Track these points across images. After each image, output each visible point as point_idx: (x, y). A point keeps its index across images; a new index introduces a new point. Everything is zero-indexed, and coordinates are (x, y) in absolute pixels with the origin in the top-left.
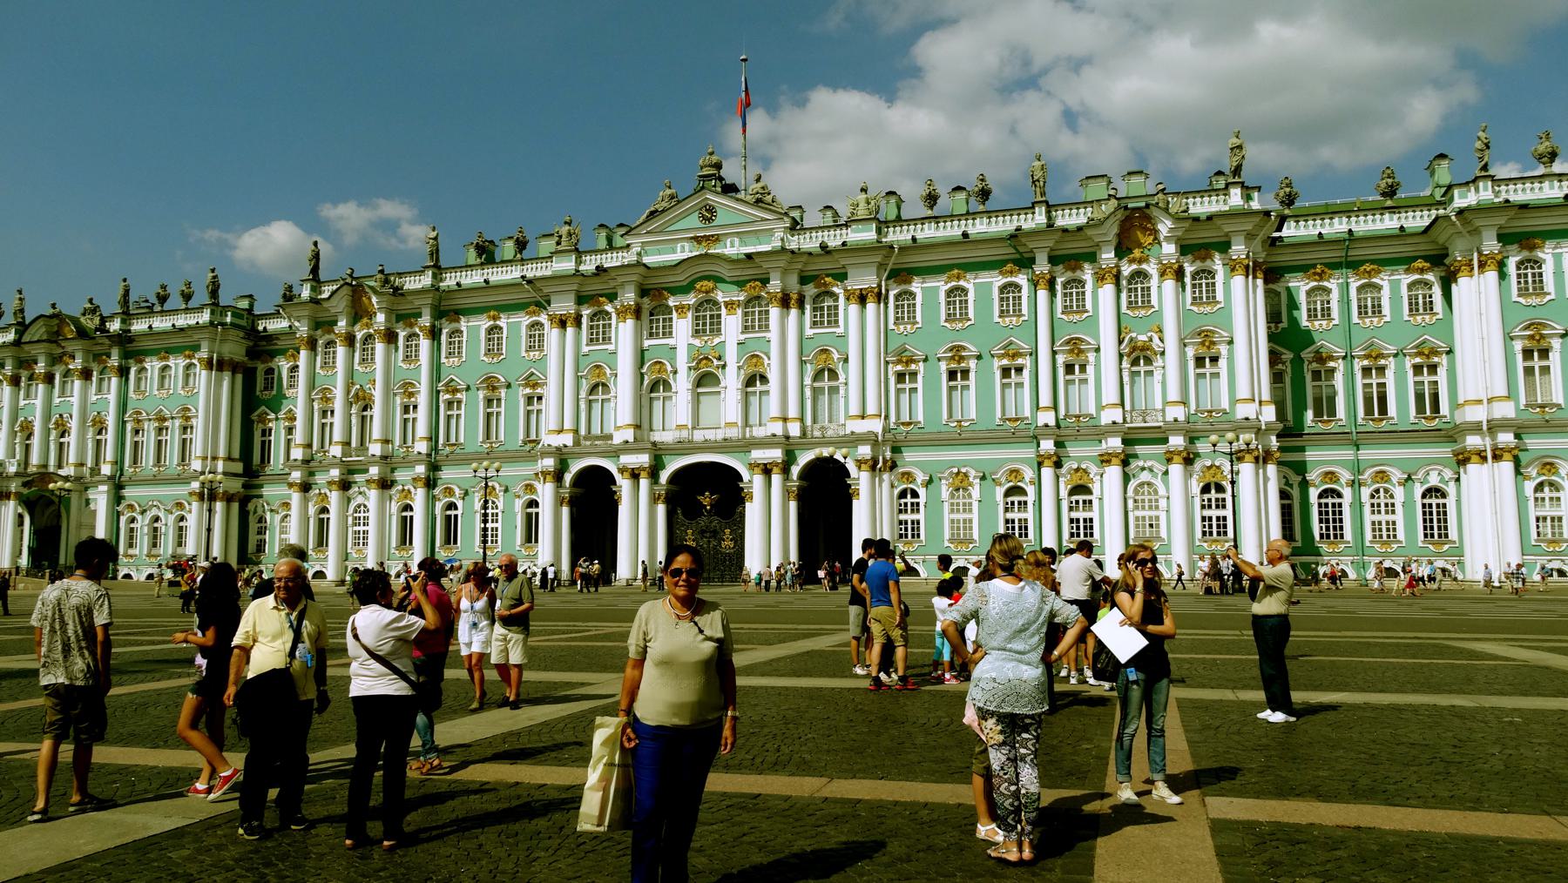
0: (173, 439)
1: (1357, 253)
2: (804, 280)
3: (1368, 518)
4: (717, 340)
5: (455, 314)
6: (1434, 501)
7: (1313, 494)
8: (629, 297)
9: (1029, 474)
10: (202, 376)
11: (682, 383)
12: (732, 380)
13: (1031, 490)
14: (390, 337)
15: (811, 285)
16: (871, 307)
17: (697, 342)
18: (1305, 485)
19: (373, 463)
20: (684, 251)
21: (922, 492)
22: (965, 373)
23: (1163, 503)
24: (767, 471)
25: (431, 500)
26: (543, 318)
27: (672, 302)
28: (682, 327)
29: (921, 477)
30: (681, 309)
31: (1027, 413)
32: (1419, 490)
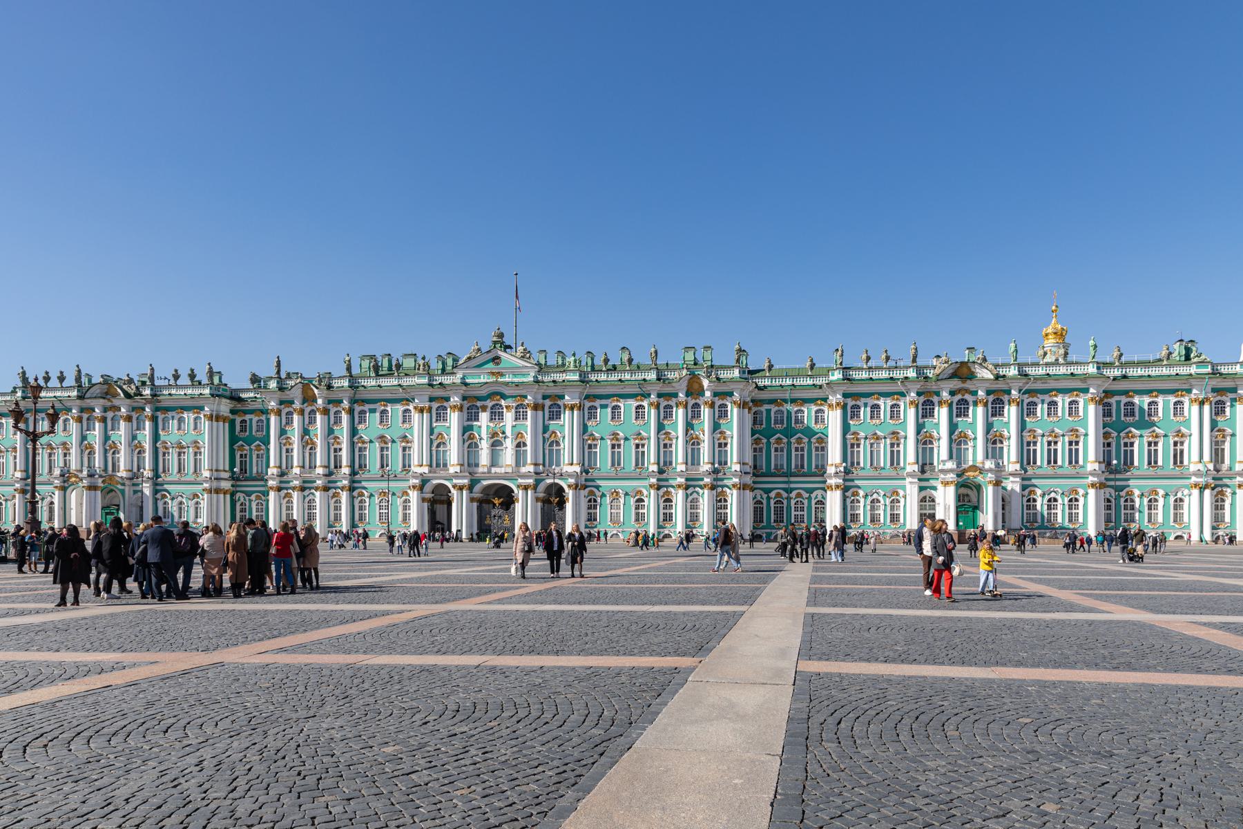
0: (189, 458)
2: (544, 397)
3: (793, 513)
7: (772, 502)
8: (455, 400)
9: (645, 492)
10: (205, 425)
14: (326, 412)
18: (769, 498)
19: (319, 478)
20: (483, 379)
22: (619, 446)
26: (411, 407)
27: (479, 404)
28: (484, 416)
30: (484, 409)
32: (813, 502)
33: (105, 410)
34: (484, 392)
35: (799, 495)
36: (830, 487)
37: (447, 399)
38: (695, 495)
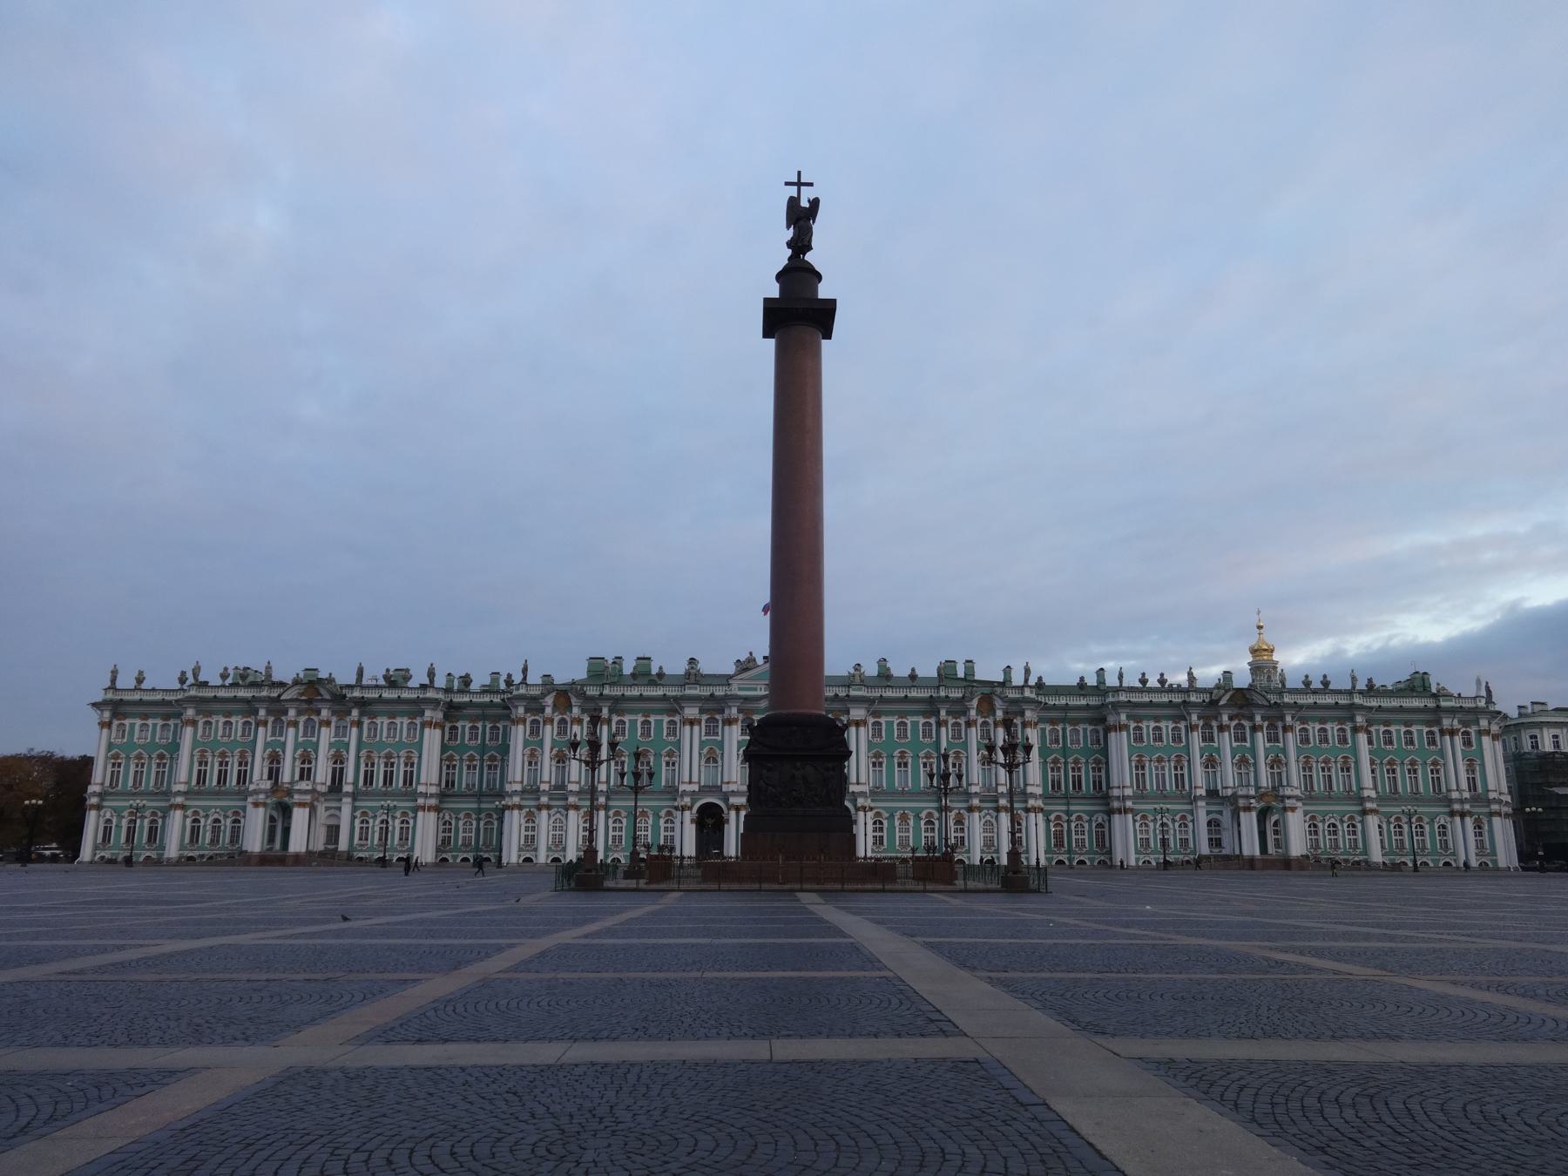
1: (1071, 714)
5: (620, 712)
16: (862, 729)
21: (885, 823)
25: (607, 817)
26: (677, 718)
33: (299, 713)
35: (1079, 818)
37: (722, 711)
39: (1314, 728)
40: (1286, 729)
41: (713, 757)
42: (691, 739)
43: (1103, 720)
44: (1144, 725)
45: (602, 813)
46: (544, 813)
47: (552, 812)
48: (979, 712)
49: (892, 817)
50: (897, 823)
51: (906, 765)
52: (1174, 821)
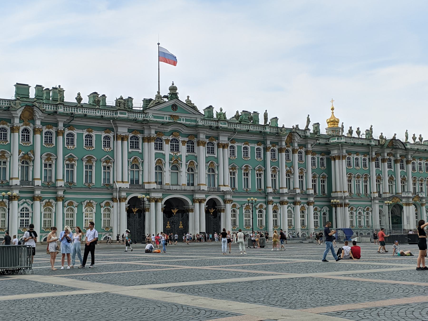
4: (179, 154)
6: (324, 216)
11: (167, 168)
12: (184, 169)
13: (264, 211)
15: (208, 139)
17: (172, 154)
21: (238, 211)
23: (293, 216)
24: (200, 201)
26: (111, 135)
27: (164, 138)
28: (167, 148)
29: (238, 206)
30: (167, 141)
31: (263, 187)
34: (170, 129)
36: (341, 205)
38: (290, 208)
39: (417, 162)
40: (408, 162)
41: (135, 165)
42: (122, 151)
43: (328, 153)
44: (351, 157)
45: (60, 203)
46: (15, 203)
47: (21, 202)
48: (286, 144)
49: (241, 208)
50: (244, 212)
51: (247, 175)
52: (364, 211)
